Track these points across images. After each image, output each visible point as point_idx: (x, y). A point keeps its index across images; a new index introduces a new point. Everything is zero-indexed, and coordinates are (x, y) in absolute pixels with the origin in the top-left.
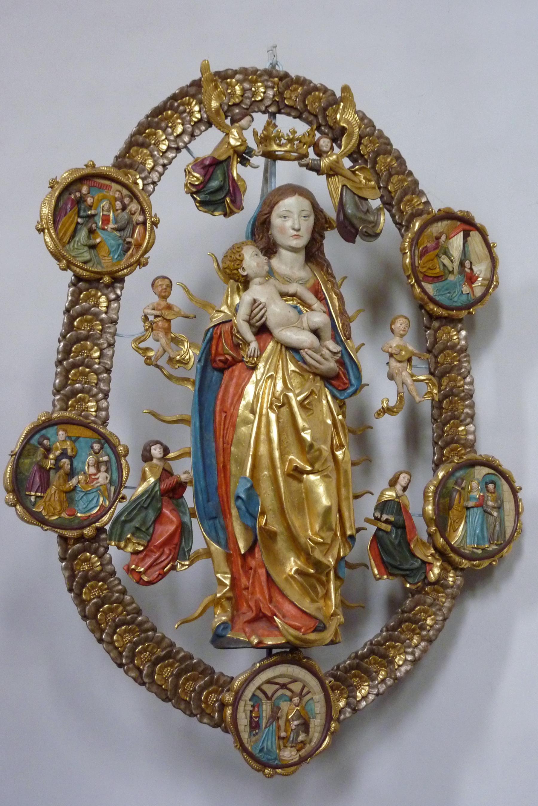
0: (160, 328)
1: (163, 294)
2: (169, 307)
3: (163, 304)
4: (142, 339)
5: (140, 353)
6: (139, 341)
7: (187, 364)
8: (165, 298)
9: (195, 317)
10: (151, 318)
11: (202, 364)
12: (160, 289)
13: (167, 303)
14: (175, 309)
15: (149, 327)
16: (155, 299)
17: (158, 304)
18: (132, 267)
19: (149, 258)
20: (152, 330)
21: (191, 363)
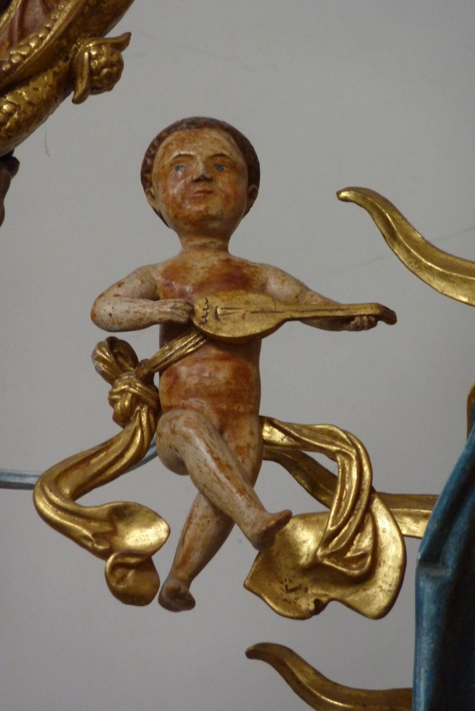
0: (188, 394)
1: (193, 208)
2: (239, 278)
3: (204, 262)
4: (97, 464)
5: (79, 540)
6: (77, 476)
7: (367, 577)
8: (210, 228)
9: (388, 316)
10: (146, 344)
11: (447, 572)
12: (175, 190)
13: (228, 261)
14: (274, 285)
15: (137, 400)
16: (167, 245)
17: (174, 271)
18: (23, 93)
19: (128, 36)
20: (157, 411)
21: (387, 573)
